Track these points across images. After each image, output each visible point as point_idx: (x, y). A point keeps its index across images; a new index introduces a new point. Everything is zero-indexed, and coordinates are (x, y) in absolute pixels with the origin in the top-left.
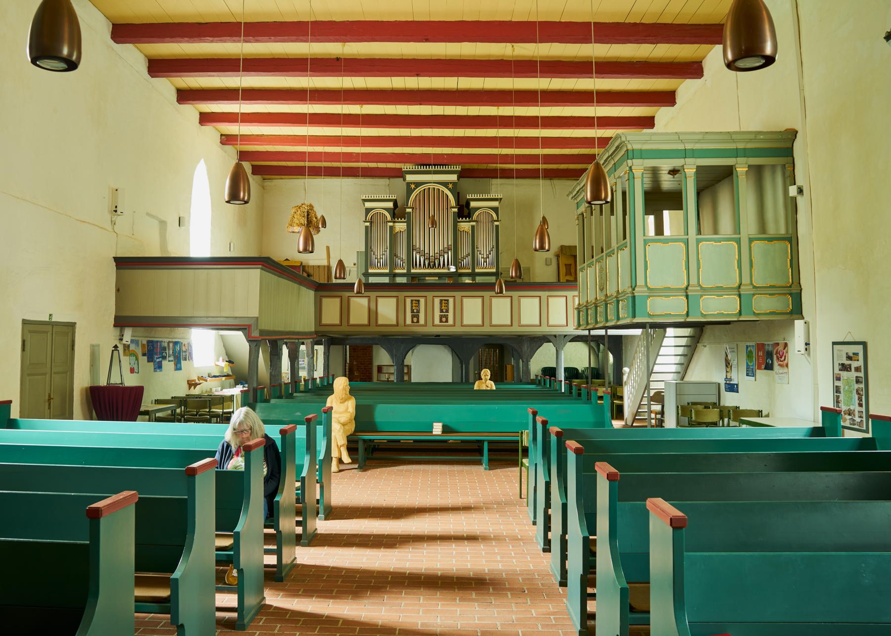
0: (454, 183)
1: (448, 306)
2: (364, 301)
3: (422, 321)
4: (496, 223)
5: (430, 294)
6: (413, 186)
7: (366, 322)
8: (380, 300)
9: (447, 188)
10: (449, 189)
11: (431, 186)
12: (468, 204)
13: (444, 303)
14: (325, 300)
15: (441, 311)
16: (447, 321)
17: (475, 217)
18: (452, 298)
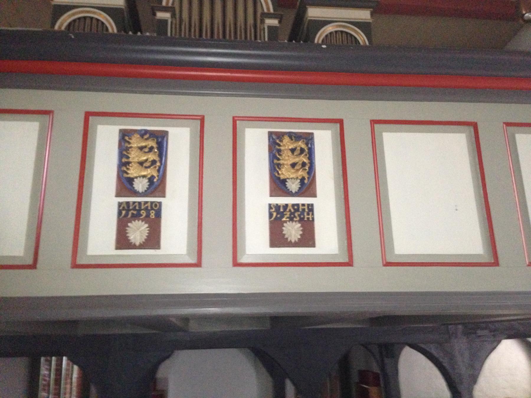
3: (176, 238)
15: (278, 186)
16: (308, 239)
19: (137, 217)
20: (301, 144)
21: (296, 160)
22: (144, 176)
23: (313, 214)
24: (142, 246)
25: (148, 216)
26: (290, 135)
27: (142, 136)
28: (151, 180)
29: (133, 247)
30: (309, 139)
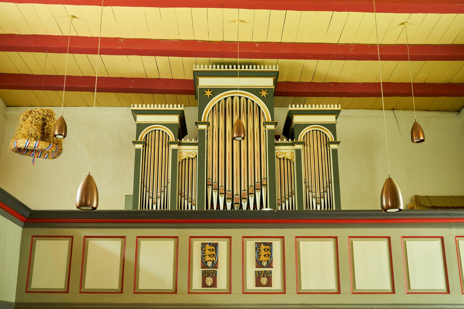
0: (268, 90)
1: (270, 256)
2: (113, 247)
3: (222, 284)
4: (333, 146)
5: (237, 233)
6: (208, 93)
7: (115, 286)
8: (144, 243)
9: (259, 96)
10: (262, 98)
11: (236, 93)
12: (289, 120)
13: (264, 249)
14: (42, 246)
15: (259, 264)
16: (269, 284)
17: (301, 138)
18: (280, 239)
19: (209, 276)
20: (268, 247)
22: (211, 261)
24: (211, 287)
25: (212, 275)
26: (264, 243)
29: (208, 287)
30: (270, 244)
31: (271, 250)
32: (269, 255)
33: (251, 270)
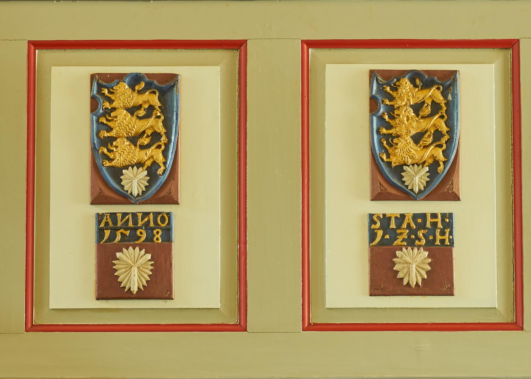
15: (388, 181)
16: (439, 281)
19: (131, 240)
20: (434, 93)
21: (424, 124)
22: (140, 165)
23: (451, 233)
25: (150, 238)
26: (415, 76)
27: (132, 87)
28: (152, 171)
29: (128, 295)
31: (448, 111)
32: (438, 135)
33: (348, 209)
